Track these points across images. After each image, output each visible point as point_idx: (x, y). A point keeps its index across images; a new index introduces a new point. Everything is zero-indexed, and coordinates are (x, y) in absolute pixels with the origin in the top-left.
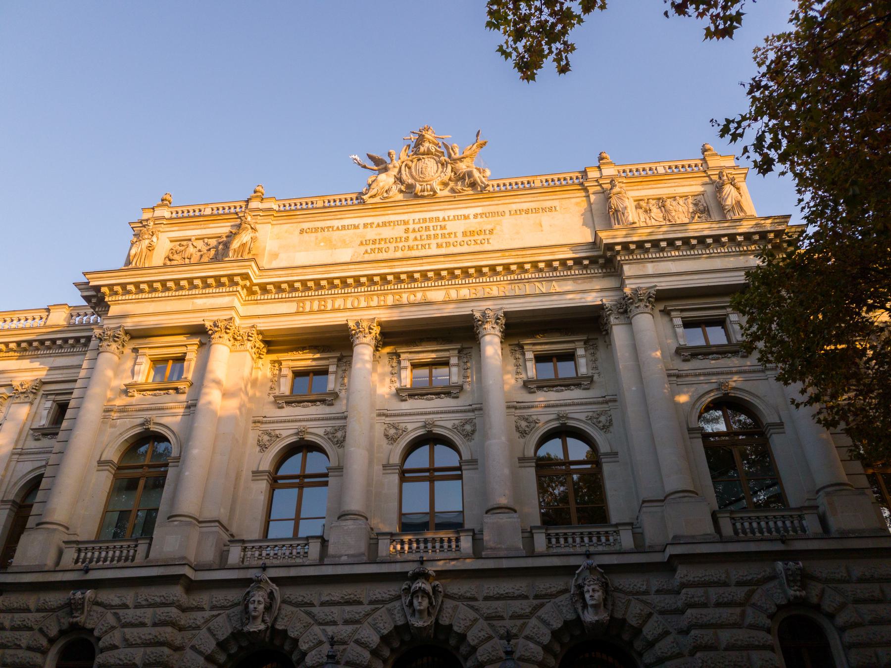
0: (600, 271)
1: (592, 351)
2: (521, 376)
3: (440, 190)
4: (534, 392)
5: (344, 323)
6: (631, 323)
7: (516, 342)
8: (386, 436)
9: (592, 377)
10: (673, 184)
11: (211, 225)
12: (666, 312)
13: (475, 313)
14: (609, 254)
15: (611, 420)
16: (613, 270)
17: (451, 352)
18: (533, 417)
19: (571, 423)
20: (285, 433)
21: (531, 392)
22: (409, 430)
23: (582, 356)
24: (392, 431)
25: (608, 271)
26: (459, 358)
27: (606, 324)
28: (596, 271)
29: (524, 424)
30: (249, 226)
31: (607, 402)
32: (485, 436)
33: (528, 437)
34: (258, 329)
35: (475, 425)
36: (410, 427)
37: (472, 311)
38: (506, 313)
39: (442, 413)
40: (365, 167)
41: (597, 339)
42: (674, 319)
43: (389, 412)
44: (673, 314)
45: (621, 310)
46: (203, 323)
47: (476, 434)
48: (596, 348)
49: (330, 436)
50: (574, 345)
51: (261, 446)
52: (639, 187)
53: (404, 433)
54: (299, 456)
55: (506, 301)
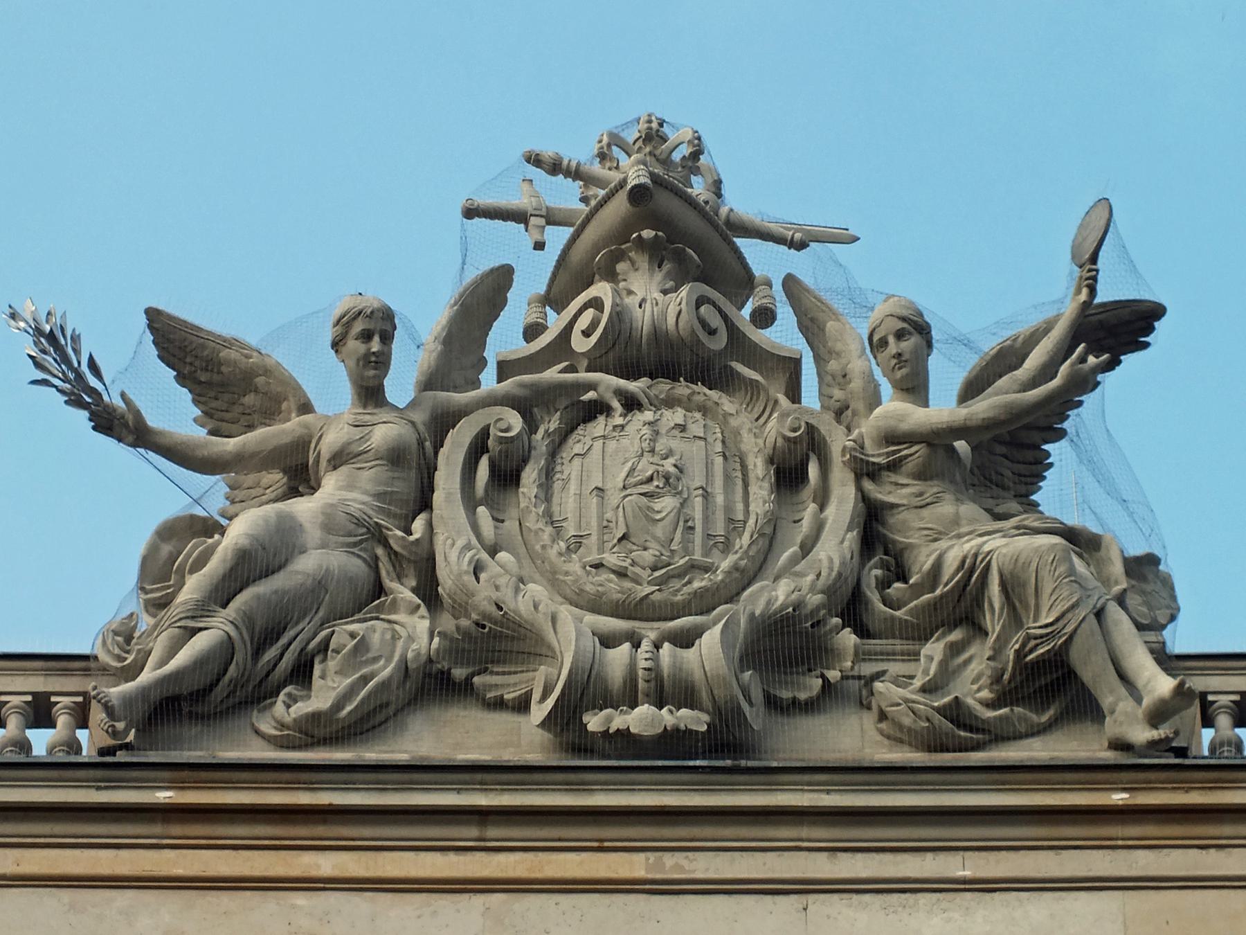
3: (773, 704)
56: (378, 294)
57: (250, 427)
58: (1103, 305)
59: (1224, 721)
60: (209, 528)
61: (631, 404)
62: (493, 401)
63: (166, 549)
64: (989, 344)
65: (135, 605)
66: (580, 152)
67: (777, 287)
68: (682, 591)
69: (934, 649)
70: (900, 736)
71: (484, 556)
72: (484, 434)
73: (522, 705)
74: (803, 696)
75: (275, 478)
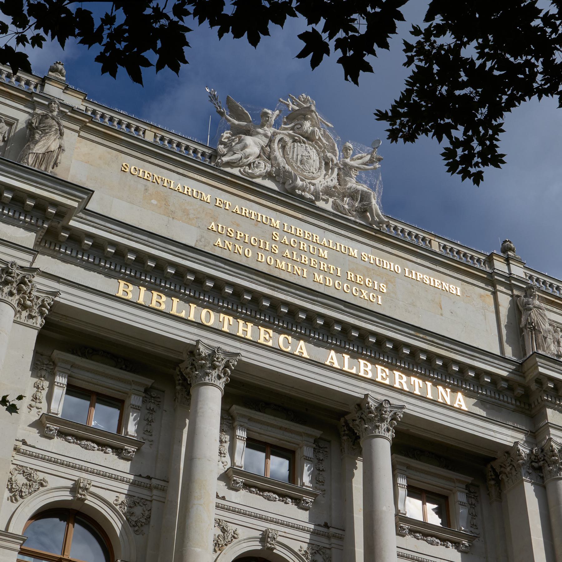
61: (304, 143)
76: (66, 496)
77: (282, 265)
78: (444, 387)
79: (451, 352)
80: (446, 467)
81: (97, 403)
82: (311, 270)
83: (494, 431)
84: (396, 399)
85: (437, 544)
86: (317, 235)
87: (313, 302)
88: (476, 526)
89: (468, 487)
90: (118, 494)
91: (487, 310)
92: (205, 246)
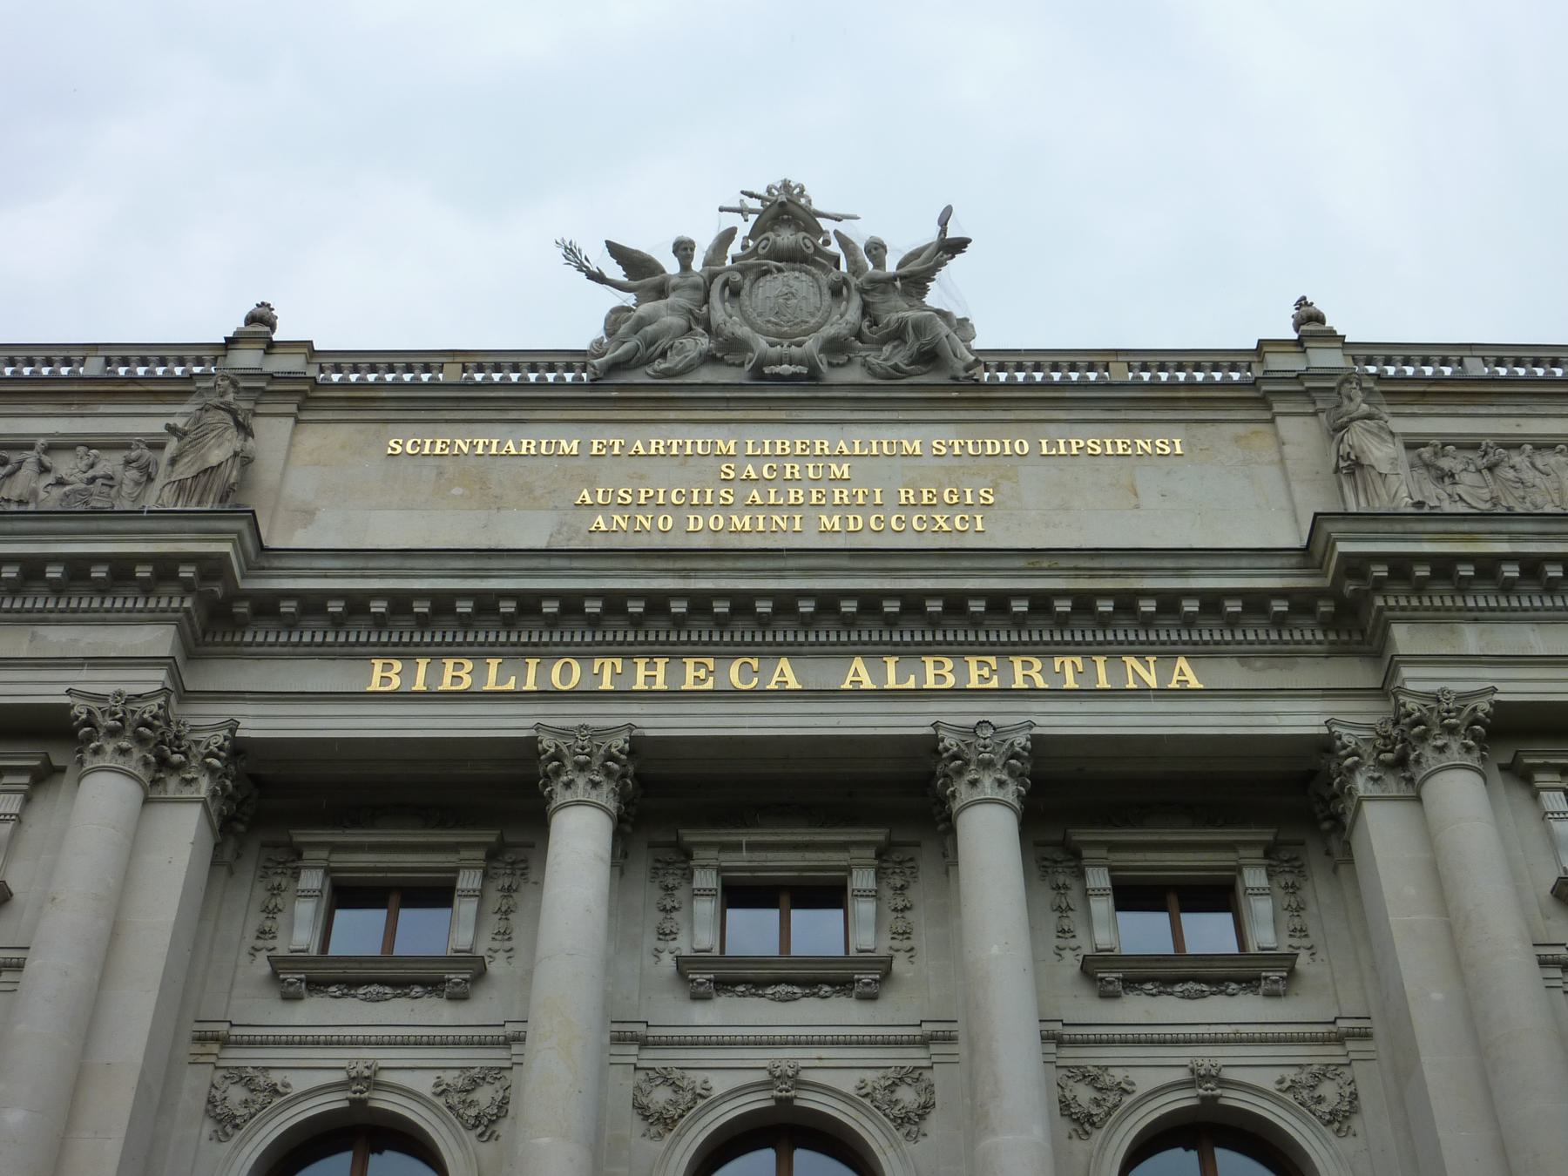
0: (1320, 636)
1: (1289, 879)
2: (1073, 943)
3: (830, 364)
4: (1115, 996)
5: (524, 734)
6: (1418, 799)
7: (1058, 837)
8: (642, 1110)
9: (1292, 957)
10: (1514, 410)
11: (102, 409)
12: (1521, 775)
13: (942, 733)
14: (1350, 587)
15: (1354, 1096)
16: (1357, 637)
17: (855, 852)
18: (1112, 1071)
19: (1234, 1099)
20: (300, 1082)
21: (1107, 995)
22: (716, 1093)
23: (1259, 893)
24: (660, 1097)
25: (1345, 637)
26: (880, 875)
27: (1335, 796)
28: (1308, 636)
29: (1084, 1095)
30: (228, 418)
31: (1340, 1039)
32: (977, 1121)
33: (1098, 1135)
34: (239, 734)
35: (929, 1088)
36: (720, 1084)
37: (935, 725)
38: (1035, 739)
39: (822, 1043)
40: (598, 277)
41: (1302, 844)
42: (1543, 794)
43: (653, 1032)
44: (1541, 779)
45: (1389, 756)
46: (66, 700)
47: (934, 1118)
48: (1300, 870)
49: (454, 1099)
50: (1232, 856)
51: (219, 1120)
52: (1415, 409)
53: (701, 1103)
54: (344, 1160)
55: (1036, 706)
56: (688, 234)
57: (644, 278)
58: (948, 239)
59: (993, 370)
60: (629, 309)
61: (780, 270)
62: (729, 269)
63: (613, 317)
64: (907, 251)
65: (603, 334)
66: (762, 191)
67: (831, 234)
68: (797, 329)
69: (887, 349)
70: (874, 374)
71: (728, 319)
72: (728, 279)
73: (742, 365)
74: (841, 362)
75: (653, 294)
76: (334, 1102)
77: (742, 522)
78: (1140, 655)
79: (1128, 577)
80: (442, 824)
81: (339, 908)
82: (812, 512)
83: (1276, 714)
84: (1005, 715)
85: (1201, 995)
86: (823, 441)
87: (779, 573)
88: (1301, 931)
89: (1270, 851)
90: (440, 1073)
91: (1256, 463)
92: (569, 540)
